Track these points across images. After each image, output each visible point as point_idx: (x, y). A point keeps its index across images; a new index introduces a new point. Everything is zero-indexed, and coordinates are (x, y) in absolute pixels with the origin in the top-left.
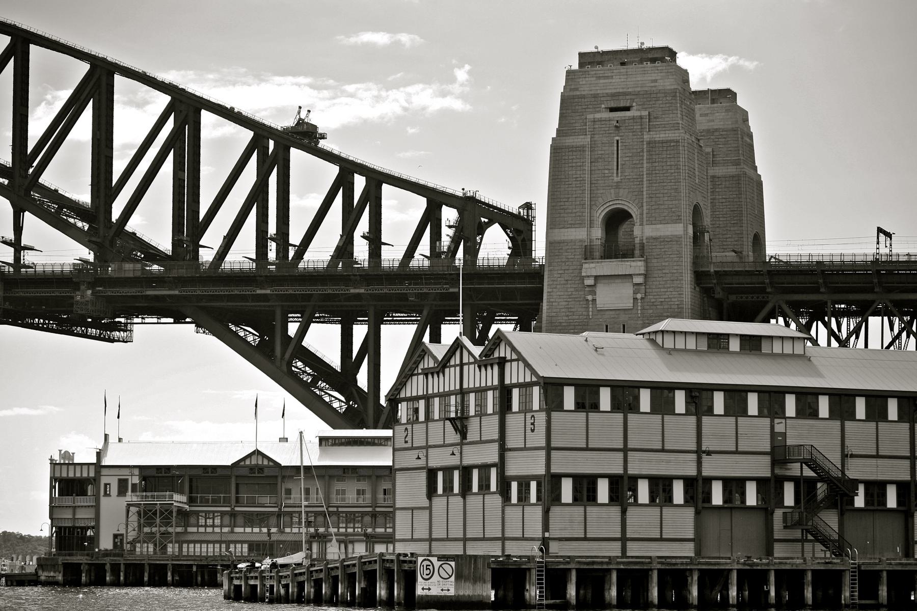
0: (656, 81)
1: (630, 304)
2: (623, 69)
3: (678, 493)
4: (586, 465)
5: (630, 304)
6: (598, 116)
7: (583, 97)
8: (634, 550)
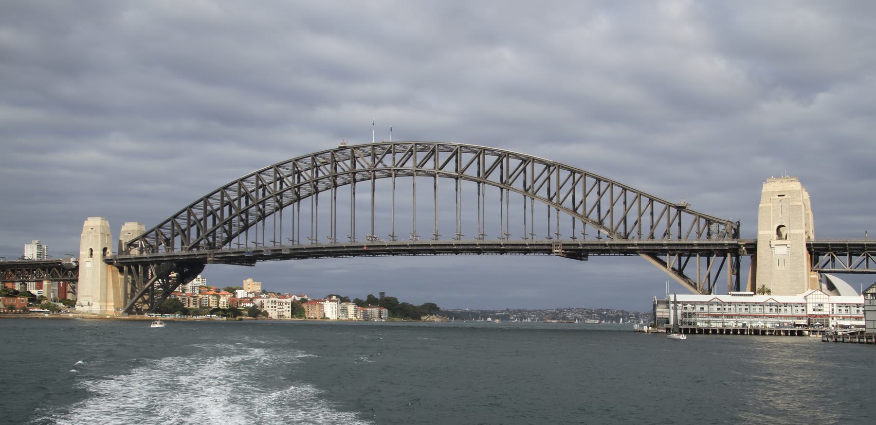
1: (786, 253)
2: (782, 184)
5: (786, 253)
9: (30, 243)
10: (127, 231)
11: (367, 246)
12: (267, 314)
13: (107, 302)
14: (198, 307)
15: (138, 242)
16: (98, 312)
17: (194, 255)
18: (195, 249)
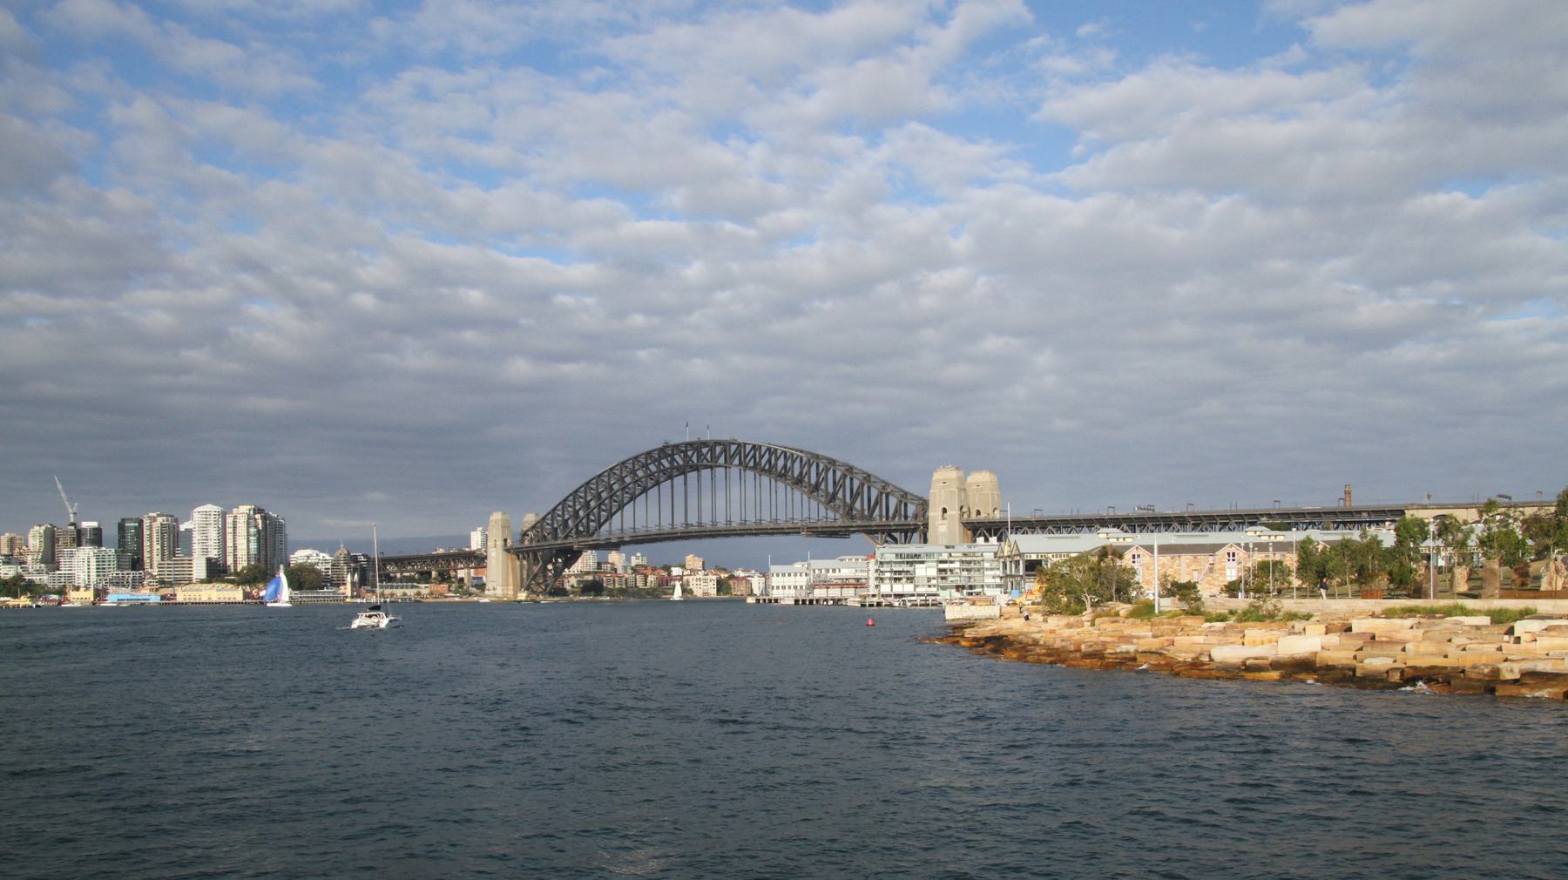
9: (475, 530)
12: (692, 592)
13: (508, 586)
14: (624, 587)
15: (529, 533)
16: (500, 596)
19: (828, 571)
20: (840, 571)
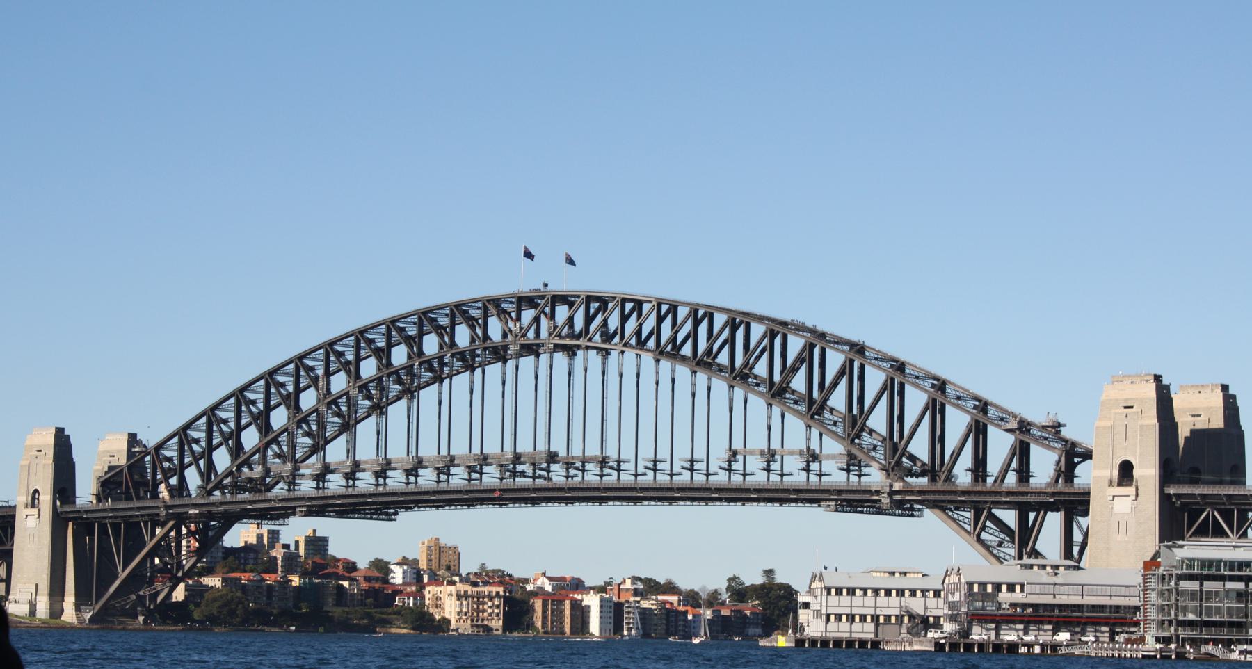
0: (1145, 393)
2: (1134, 386)
3: (869, 618)
4: (839, 611)
6: (1117, 411)
7: (1111, 400)
8: (854, 635)
10: (108, 452)
11: (500, 490)
17: (213, 504)
18: (217, 493)
19: (998, 587)
20: (1022, 590)
